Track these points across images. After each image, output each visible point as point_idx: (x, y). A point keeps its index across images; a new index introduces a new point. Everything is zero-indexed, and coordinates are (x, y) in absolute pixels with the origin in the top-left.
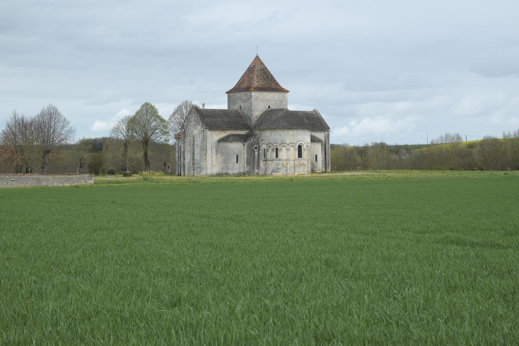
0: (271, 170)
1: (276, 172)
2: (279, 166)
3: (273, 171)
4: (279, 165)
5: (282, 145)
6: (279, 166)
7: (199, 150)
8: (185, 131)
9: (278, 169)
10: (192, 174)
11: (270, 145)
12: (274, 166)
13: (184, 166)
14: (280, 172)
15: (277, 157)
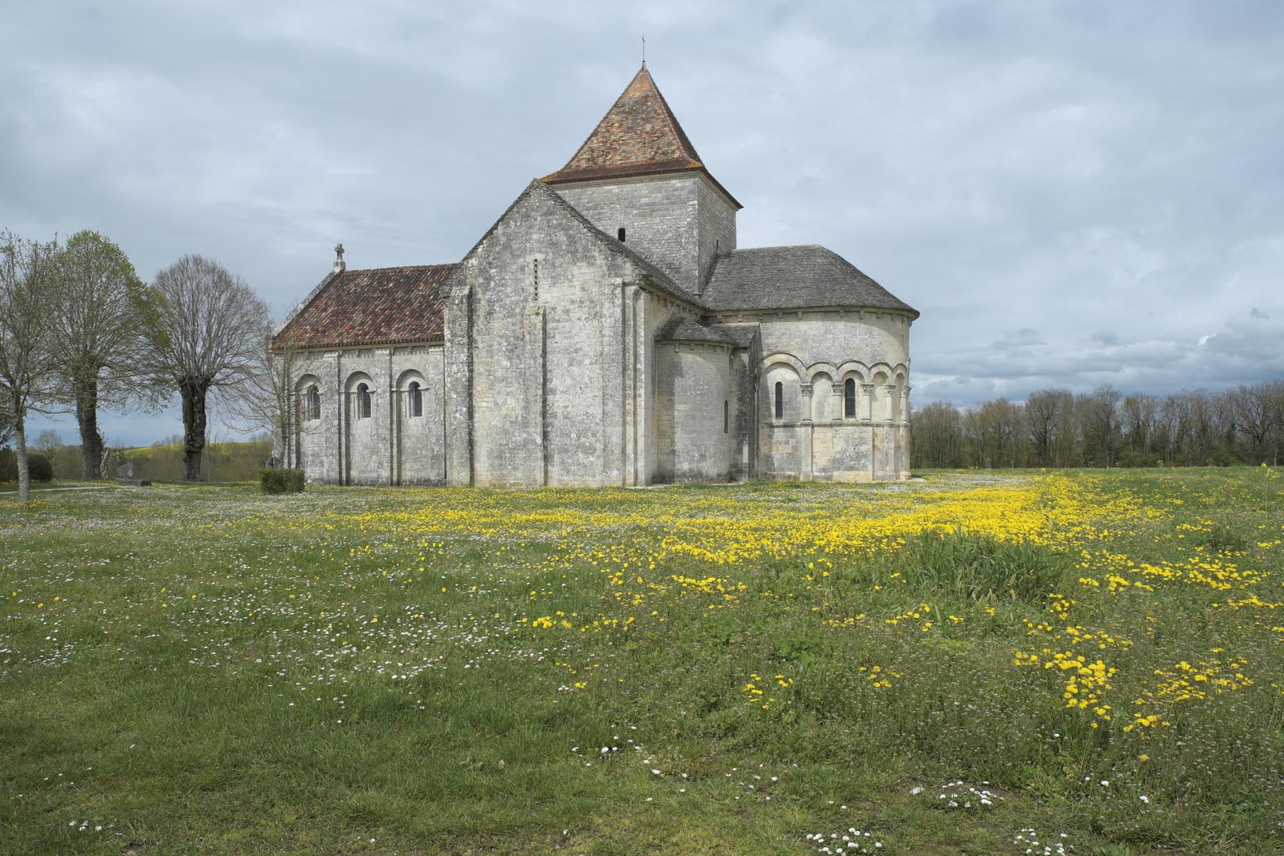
0: (822, 460)
1: (852, 468)
2: (864, 448)
3: (837, 463)
4: (862, 441)
5: (875, 370)
6: (864, 448)
7: (589, 372)
8: (471, 295)
9: (859, 456)
10: (539, 476)
11: (825, 368)
12: (840, 445)
13: (471, 444)
14: (864, 467)
15: (850, 410)
